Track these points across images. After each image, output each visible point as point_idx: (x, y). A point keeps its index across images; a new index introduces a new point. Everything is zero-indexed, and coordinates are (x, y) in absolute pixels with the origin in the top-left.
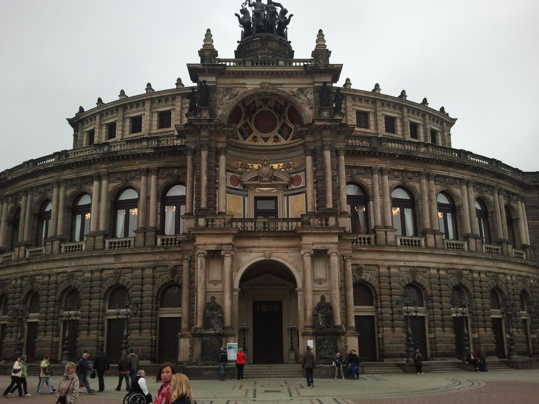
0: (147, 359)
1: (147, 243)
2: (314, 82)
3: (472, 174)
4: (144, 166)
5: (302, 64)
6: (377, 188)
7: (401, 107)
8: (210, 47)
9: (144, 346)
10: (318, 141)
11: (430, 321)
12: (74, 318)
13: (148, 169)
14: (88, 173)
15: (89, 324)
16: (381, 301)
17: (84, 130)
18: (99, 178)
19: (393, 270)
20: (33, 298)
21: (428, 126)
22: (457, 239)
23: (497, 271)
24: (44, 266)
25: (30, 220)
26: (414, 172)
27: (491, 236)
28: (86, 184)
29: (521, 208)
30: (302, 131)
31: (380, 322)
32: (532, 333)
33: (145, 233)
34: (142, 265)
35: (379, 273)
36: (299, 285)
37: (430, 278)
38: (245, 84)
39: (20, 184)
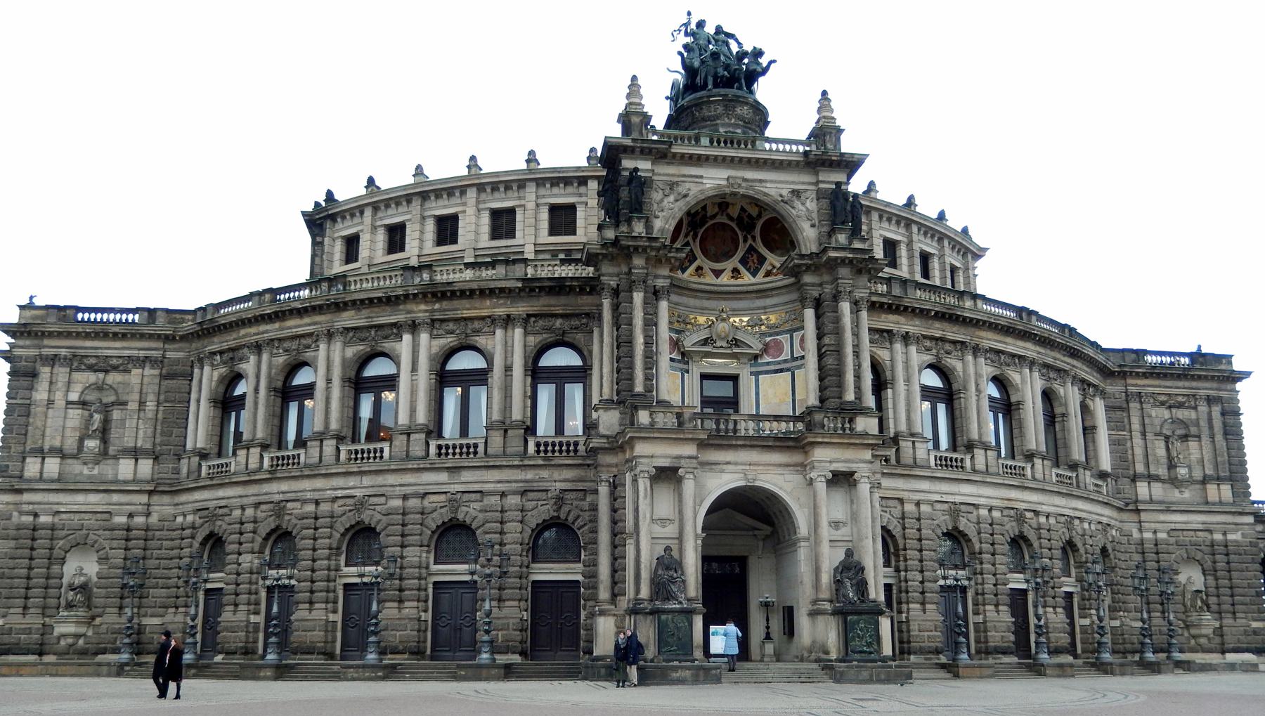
0: (514, 653)
1: (509, 450)
2: (818, 182)
3: (1038, 348)
4: (501, 311)
5: (801, 149)
7: (909, 223)
8: (638, 109)
9: (508, 629)
10: (827, 283)
11: (977, 594)
12: (287, 582)
13: (508, 316)
14: (393, 319)
15: (401, 590)
16: (906, 560)
17: (336, 235)
18: (414, 327)
19: (924, 508)
20: (281, 539)
21: (949, 260)
22: (1013, 458)
23: (1071, 513)
24: (306, 484)
25: (267, 400)
26: (954, 342)
27: (1056, 451)
28: (386, 338)
29: (1098, 406)
30: (799, 266)
31: (903, 594)
32: (1111, 619)
33: (506, 431)
35: (903, 513)
36: (803, 527)
37: (978, 523)
38: (701, 177)
39: (243, 332)
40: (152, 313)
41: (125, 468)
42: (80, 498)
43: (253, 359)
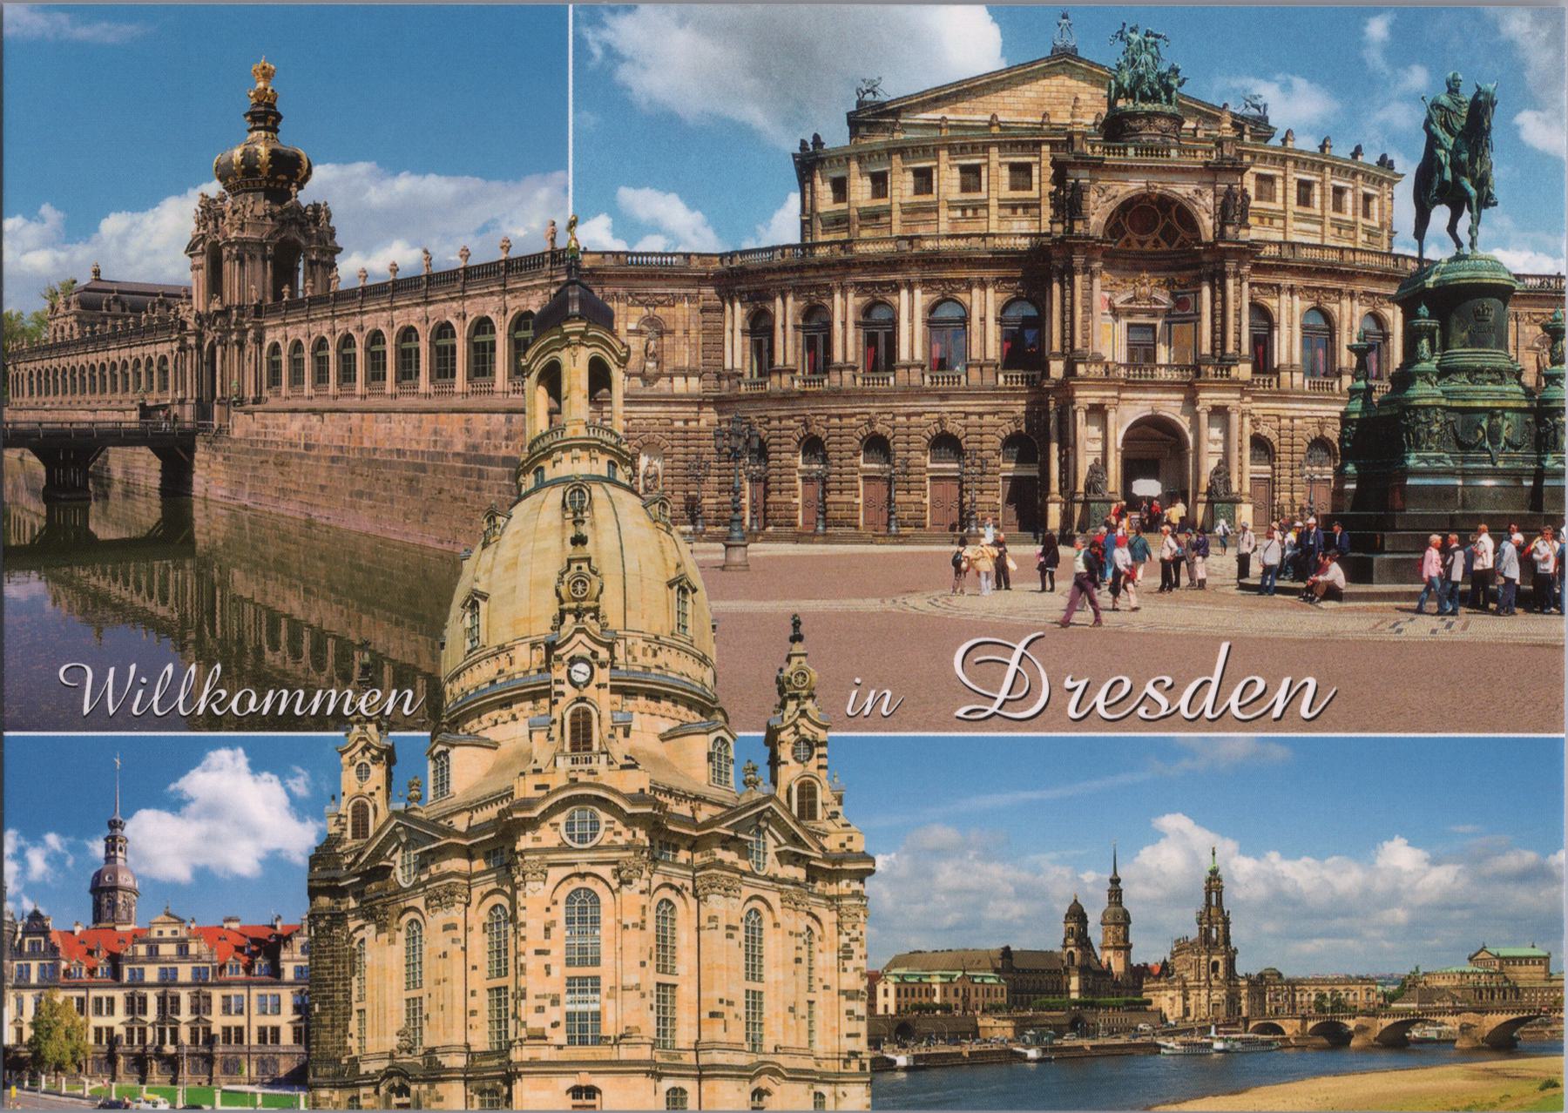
6: (1284, 313)
34: (981, 409)
40: (687, 256)
41: (679, 385)
42: (648, 408)
43: (779, 301)
